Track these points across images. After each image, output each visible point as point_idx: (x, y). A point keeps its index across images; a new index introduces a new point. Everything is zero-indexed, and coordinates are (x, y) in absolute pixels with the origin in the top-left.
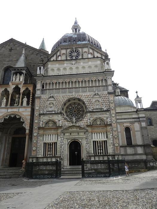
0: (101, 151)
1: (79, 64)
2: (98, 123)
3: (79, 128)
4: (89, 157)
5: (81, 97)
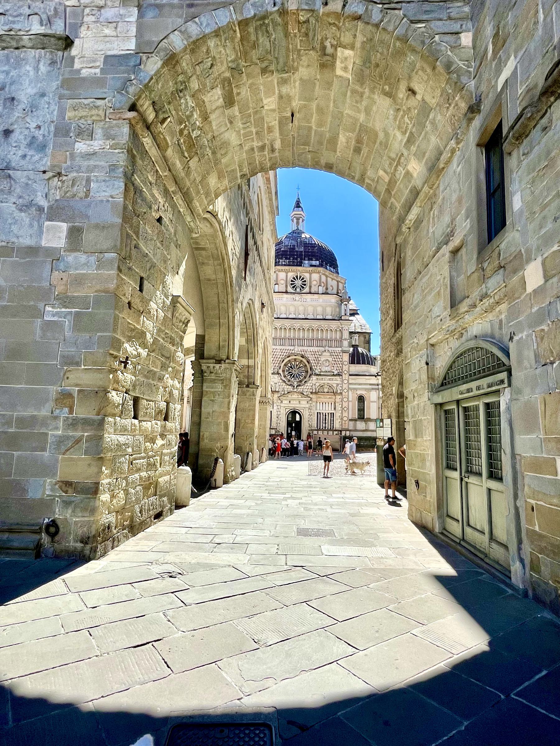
2: (326, 390)
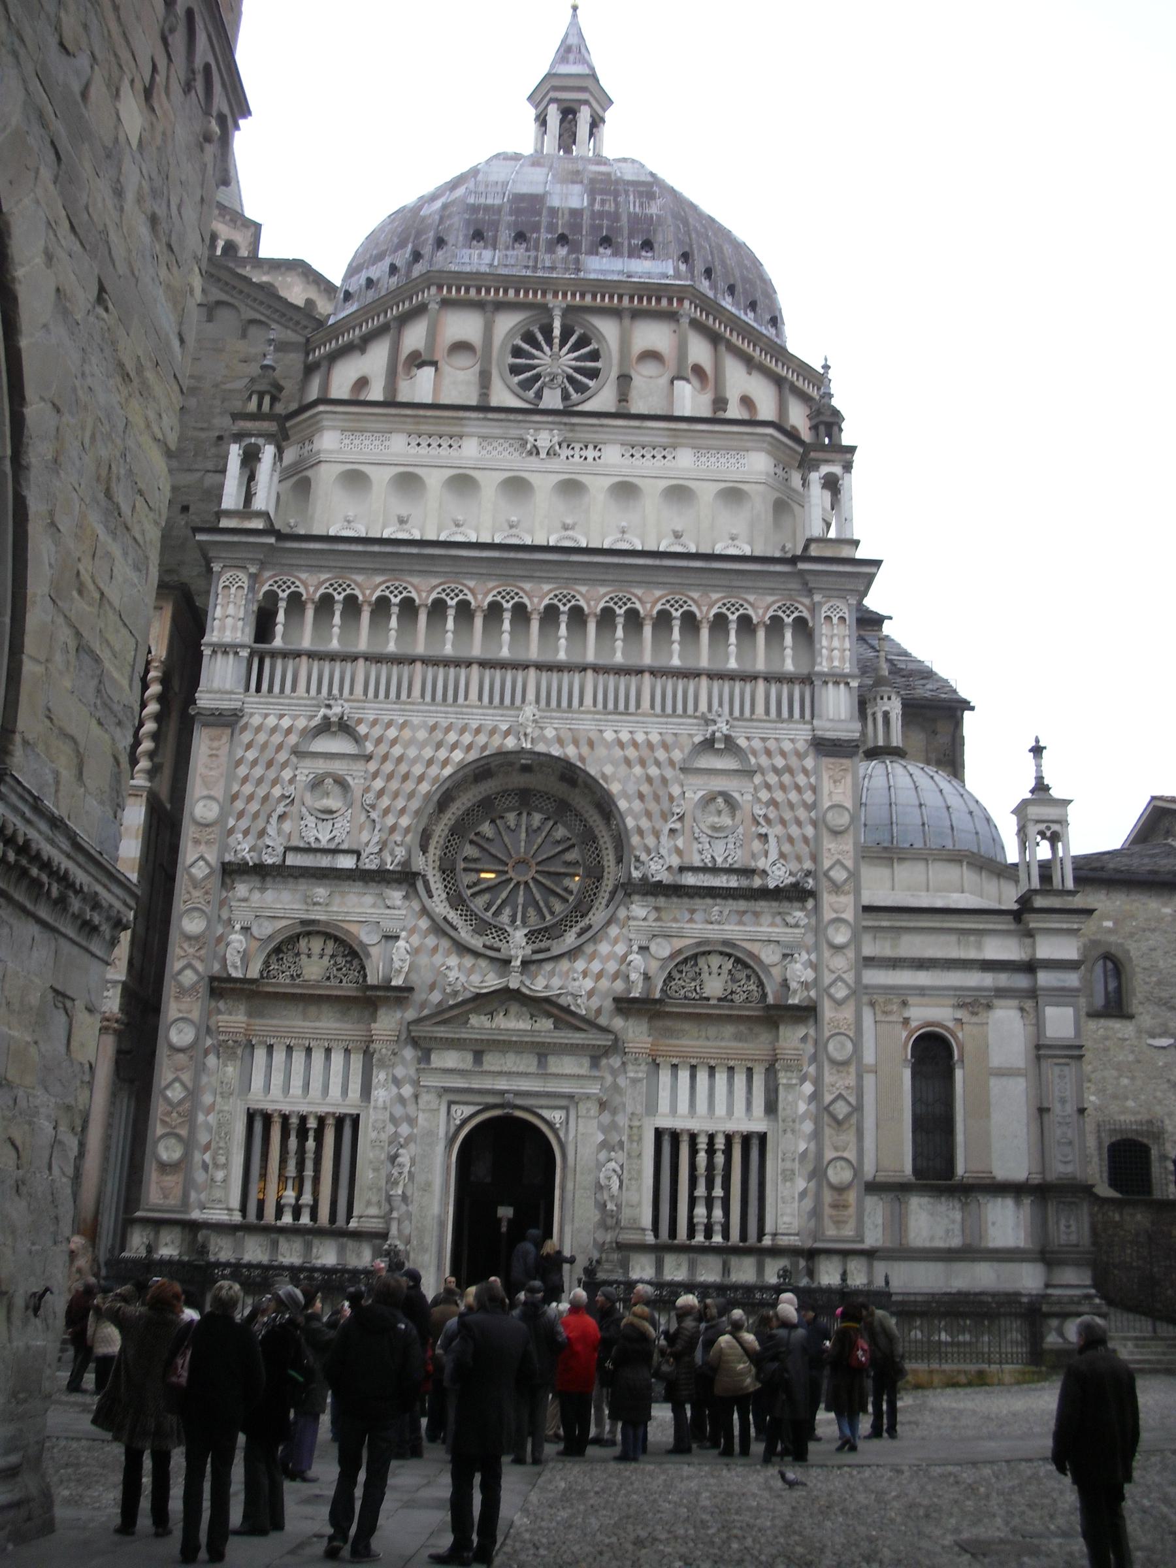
0: (709, 1216)
1: (590, 453)
2: (714, 987)
3: (549, 1015)
4: (615, 1256)
5: (585, 750)
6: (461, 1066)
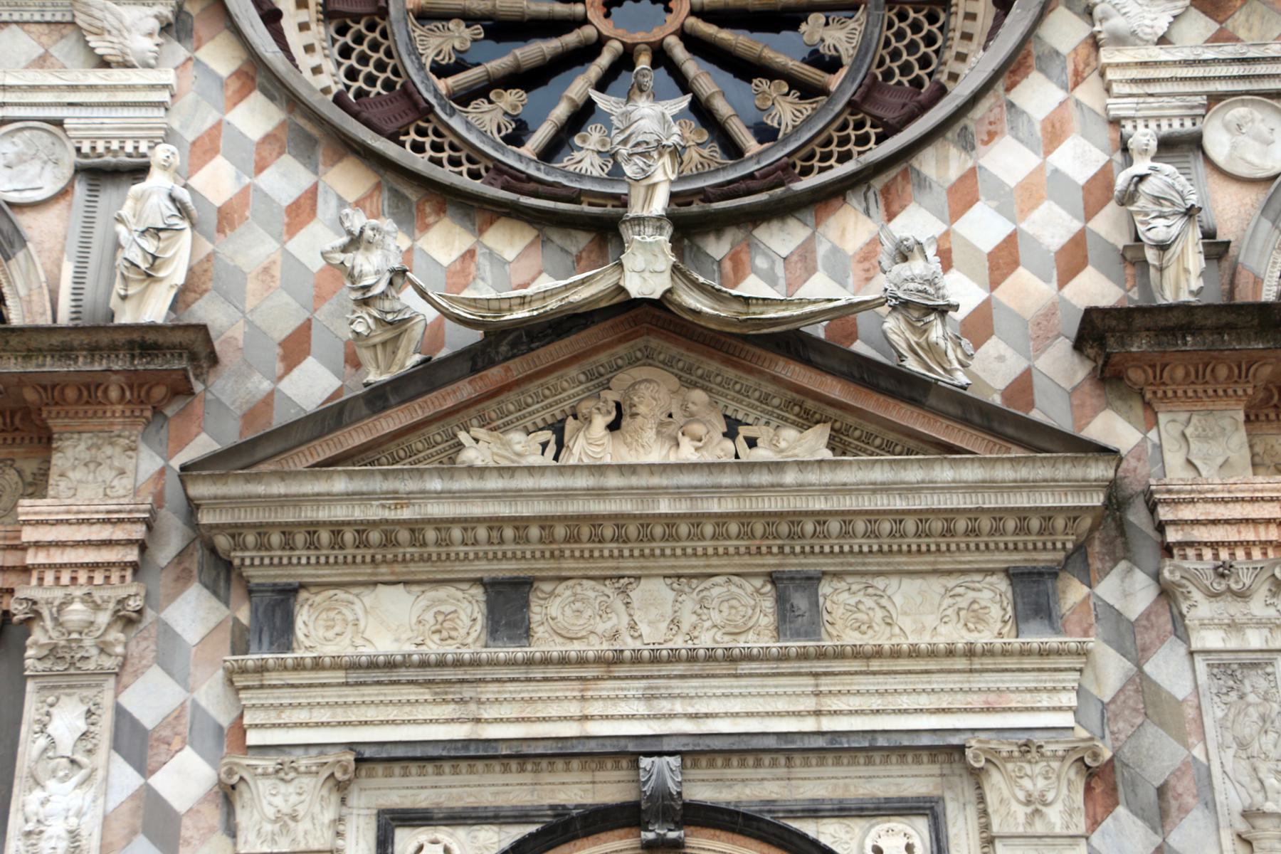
6: (434, 648)
